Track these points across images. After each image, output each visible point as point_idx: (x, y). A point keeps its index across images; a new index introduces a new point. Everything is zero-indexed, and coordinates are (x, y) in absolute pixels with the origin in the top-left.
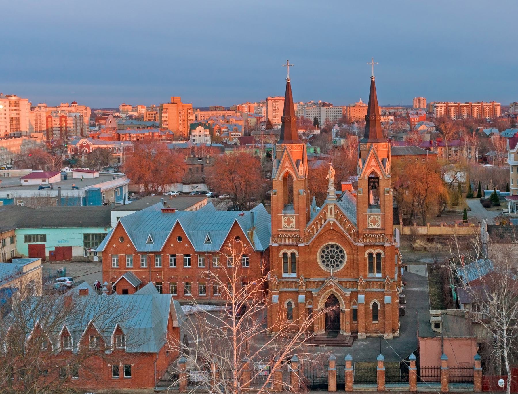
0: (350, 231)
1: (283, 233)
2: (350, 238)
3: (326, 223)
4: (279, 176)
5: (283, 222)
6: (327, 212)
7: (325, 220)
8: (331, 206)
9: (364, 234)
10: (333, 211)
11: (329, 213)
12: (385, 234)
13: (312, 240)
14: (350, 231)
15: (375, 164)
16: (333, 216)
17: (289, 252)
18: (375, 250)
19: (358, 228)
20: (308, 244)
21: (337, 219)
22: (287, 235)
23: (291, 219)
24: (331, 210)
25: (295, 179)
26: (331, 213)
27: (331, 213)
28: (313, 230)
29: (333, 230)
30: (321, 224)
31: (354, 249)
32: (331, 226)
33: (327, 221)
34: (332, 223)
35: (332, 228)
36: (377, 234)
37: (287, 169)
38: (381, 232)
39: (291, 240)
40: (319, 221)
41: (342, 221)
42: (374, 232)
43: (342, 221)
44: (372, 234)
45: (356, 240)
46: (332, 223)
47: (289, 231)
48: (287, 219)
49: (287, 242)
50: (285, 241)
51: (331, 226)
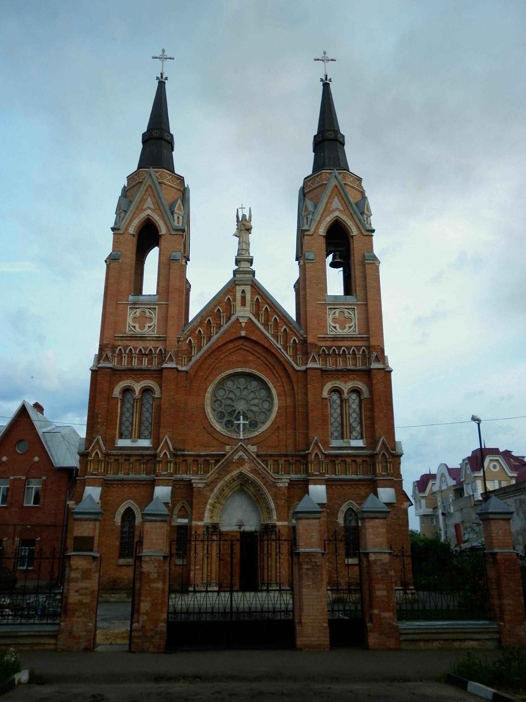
0: (286, 341)
1: (127, 343)
3: (230, 322)
4: (129, 225)
5: (129, 320)
7: (229, 318)
8: (242, 287)
9: (320, 347)
10: (248, 296)
14: (286, 341)
15: (341, 208)
16: (248, 308)
17: (138, 387)
19: (306, 333)
20: (184, 369)
21: (257, 315)
23: (148, 314)
24: (243, 299)
26: (243, 304)
27: (243, 304)
28: (199, 337)
29: (245, 338)
30: (219, 327)
31: (294, 379)
32: (241, 328)
33: (233, 318)
34: (243, 321)
35: (243, 333)
36: (349, 348)
38: (359, 343)
39: (145, 361)
40: (214, 319)
41: (267, 320)
43: (267, 320)
45: (299, 361)
46: (243, 321)
47: (142, 338)
49: (135, 364)
50: (130, 362)
51: (241, 328)
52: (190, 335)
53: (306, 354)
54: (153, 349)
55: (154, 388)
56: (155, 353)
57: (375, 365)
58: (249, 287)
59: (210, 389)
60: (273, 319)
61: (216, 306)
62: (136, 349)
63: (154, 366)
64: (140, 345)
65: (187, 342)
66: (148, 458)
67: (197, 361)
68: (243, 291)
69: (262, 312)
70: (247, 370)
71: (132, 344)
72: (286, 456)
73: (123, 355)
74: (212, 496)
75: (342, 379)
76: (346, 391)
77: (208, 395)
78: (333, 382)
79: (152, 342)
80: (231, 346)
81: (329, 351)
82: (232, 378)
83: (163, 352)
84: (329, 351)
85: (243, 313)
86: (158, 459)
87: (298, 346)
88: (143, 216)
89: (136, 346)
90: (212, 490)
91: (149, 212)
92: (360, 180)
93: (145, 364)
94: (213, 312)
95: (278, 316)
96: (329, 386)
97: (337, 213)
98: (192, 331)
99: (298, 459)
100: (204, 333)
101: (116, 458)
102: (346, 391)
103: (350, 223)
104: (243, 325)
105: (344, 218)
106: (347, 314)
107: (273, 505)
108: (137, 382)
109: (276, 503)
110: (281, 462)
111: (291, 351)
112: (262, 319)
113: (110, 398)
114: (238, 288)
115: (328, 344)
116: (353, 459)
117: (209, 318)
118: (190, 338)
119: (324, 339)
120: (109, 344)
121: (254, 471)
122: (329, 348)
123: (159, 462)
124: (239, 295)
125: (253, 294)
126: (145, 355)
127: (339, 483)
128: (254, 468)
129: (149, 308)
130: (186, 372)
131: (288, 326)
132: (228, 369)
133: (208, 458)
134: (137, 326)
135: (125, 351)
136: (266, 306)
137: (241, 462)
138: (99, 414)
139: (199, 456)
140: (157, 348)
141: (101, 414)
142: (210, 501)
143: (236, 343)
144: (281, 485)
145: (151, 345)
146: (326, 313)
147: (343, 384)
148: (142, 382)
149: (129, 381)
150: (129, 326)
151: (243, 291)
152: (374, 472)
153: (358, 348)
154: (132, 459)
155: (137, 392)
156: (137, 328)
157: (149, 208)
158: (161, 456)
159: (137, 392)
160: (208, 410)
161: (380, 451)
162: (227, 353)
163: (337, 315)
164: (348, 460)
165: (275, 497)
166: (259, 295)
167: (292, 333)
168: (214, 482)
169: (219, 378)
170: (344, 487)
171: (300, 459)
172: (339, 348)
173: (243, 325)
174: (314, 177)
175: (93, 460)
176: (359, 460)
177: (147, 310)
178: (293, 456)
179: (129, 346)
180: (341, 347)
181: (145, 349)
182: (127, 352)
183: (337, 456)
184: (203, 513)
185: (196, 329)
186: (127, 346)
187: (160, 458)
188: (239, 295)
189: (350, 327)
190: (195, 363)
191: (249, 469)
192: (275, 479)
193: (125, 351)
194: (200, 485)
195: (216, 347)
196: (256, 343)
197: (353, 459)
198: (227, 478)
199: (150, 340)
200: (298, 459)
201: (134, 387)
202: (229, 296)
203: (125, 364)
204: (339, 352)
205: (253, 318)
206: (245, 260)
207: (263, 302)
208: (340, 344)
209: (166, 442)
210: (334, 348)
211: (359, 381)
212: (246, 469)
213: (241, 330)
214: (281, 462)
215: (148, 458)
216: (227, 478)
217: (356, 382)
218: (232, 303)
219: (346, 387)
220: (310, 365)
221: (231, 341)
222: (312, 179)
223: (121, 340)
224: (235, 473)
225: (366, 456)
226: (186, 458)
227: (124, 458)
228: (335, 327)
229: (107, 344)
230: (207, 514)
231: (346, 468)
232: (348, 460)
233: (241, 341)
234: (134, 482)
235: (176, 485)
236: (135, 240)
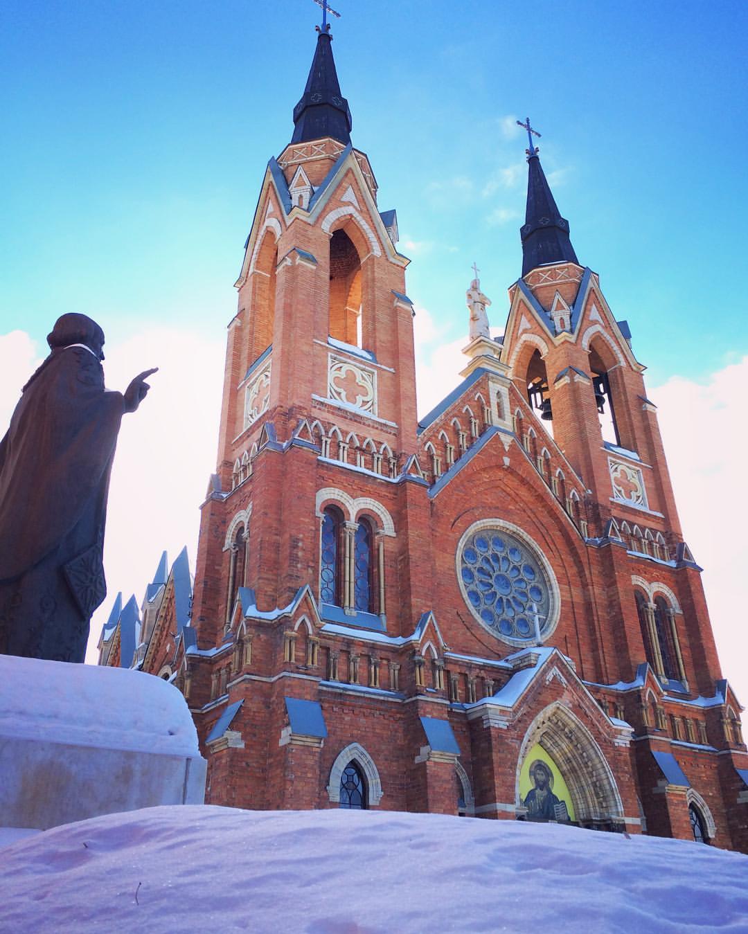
2: (566, 516)
11: (494, 409)
12: (664, 534)
22: (345, 433)
23: (359, 379)
25: (377, 252)
26: (501, 416)
27: (501, 416)
33: (489, 432)
36: (643, 529)
37: (350, 210)
47: (356, 418)
48: (342, 374)
52: (429, 440)
54: (373, 444)
55: (382, 516)
56: (378, 451)
58: (507, 389)
60: (543, 452)
62: (345, 433)
65: (426, 449)
69: (526, 437)
71: (339, 425)
73: (324, 439)
75: (644, 575)
79: (373, 432)
80: (485, 477)
83: (391, 455)
86: (417, 658)
87: (579, 506)
89: (344, 428)
94: (460, 411)
100: (451, 442)
104: (507, 448)
108: (354, 497)
109: (617, 778)
111: (570, 510)
117: (455, 419)
118: (429, 443)
120: (306, 409)
123: (420, 664)
128: (576, 703)
135: (327, 432)
136: (531, 428)
140: (381, 443)
141: (302, 540)
145: (371, 436)
146: (608, 466)
147: (646, 583)
148: (362, 500)
150: (331, 391)
153: (654, 531)
157: (350, 204)
158: (423, 654)
167: (570, 482)
172: (632, 525)
173: (507, 448)
174: (555, 269)
175: (296, 638)
177: (358, 373)
179: (334, 425)
180: (634, 524)
181: (362, 439)
182: (330, 435)
185: (438, 432)
187: (421, 655)
191: (570, 705)
193: (327, 432)
196: (523, 481)
199: (369, 426)
201: (347, 505)
202: (478, 394)
204: (632, 531)
208: (632, 518)
210: (624, 522)
211: (663, 583)
213: (504, 455)
218: (486, 408)
221: (484, 470)
222: (549, 270)
223: (320, 409)
229: (300, 407)
233: (501, 474)
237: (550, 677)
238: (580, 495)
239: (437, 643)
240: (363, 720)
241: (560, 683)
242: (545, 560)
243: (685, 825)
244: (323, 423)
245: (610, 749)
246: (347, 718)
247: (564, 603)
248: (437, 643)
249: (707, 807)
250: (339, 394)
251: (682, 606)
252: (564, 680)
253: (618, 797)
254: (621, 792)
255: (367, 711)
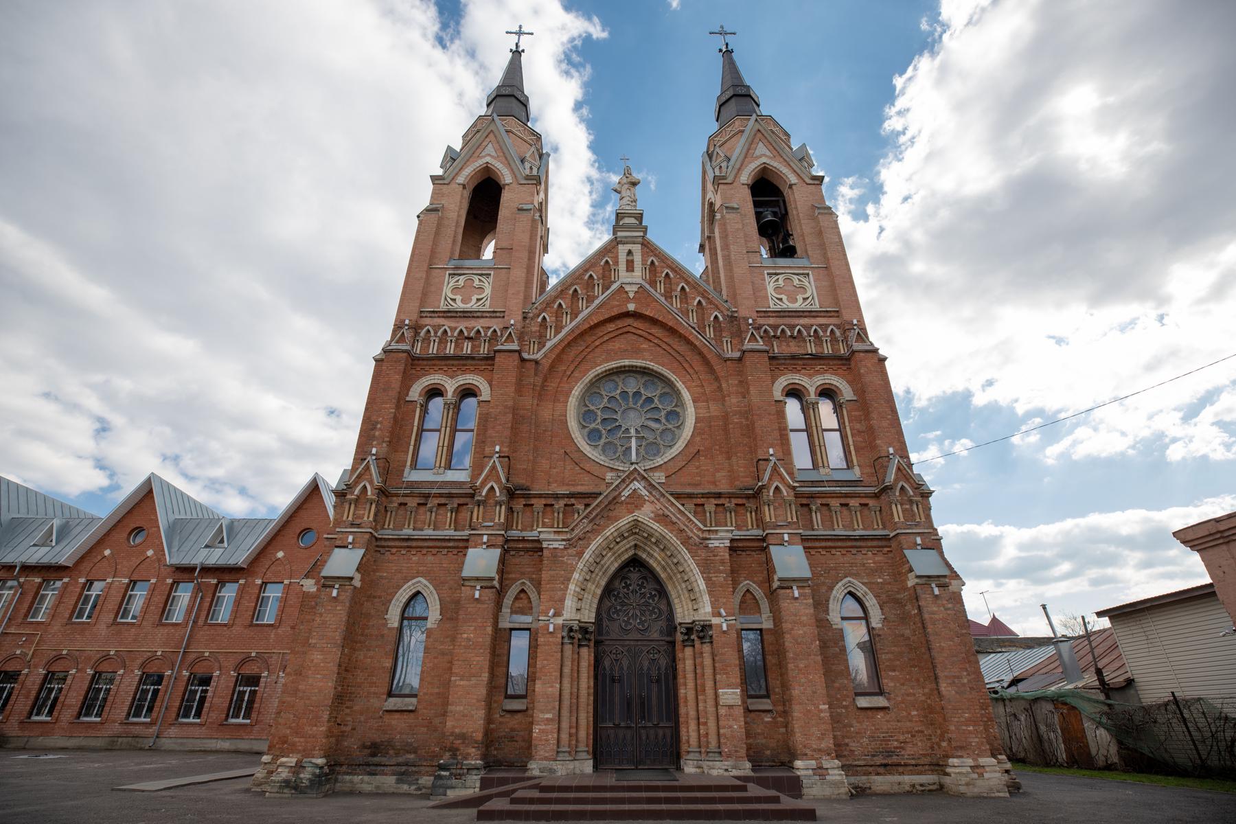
6: (616, 263)
7: (606, 288)
10: (637, 258)
11: (622, 266)
13: (549, 345)
17: (451, 386)
18: (810, 376)
21: (653, 283)
26: (630, 266)
27: (630, 266)
29: (635, 315)
31: (721, 374)
33: (614, 287)
34: (631, 290)
35: (631, 307)
36: (808, 327)
42: (796, 321)
44: (792, 327)
46: (631, 290)
49: (450, 349)
51: (629, 300)
52: (544, 310)
53: (738, 334)
57: (857, 346)
59: (577, 391)
61: (586, 271)
63: (484, 350)
64: (462, 325)
65: (540, 320)
66: (462, 501)
67: (555, 346)
68: (630, 253)
70: (639, 363)
71: (447, 324)
72: (719, 495)
74: (580, 565)
76: (812, 390)
77: (573, 402)
78: (789, 376)
80: (611, 327)
81: (775, 331)
82: (615, 377)
84: (775, 331)
85: (631, 279)
88: (478, 164)
89: (453, 325)
90: (580, 554)
91: (488, 159)
92: (788, 136)
93: (467, 348)
95: (688, 283)
96: (782, 382)
97: (764, 160)
98: (548, 304)
99: (740, 501)
101: (401, 500)
102: (812, 390)
103: (785, 170)
104: (631, 295)
105: (776, 164)
106: (796, 282)
107: (702, 584)
108: (452, 377)
109: (708, 580)
110: (710, 506)
111: (710, 333)
112: (661, 288)
113: (401, 401)
114: (620, 247)
115: (772, 321)
116: (843, 501)
119: (766, 314)
121: (662, 518)
122: (775, 327)
124: (622, 258)
125: (644, 256)
126: (469, 338)
127: (823, 544)
129: (481, 275)
130: (536, 362)
131: (704, 297)
132: (607, 361)
133: (573, 501)
134: (458, 298)
135: (436, 333)
137: (636, 501)
138: (377, 423)
139: (557, 497)
141: (381, 423)
142: (576, 575)
143: (620, 323)
144: (716, 543)
145: (479, 324)
148: (460, 378)
149: (437, 376)
151: (630, 253)
152: (887, 521)
153: (824, 327)
154: (432, 502)
155: (450, 394)
156: (459, 302)
159: (450, 394)
160: (573, 424)
161: (897, 480)
162: (606, 338)
163: (781, 282)
164: (835, 503)
165: (706, 567)
166: (655, 255)
168: (585, 538)
169: (591, 375)
170: (833, 551)
171: (744, 501)
172: (792, 327)
173: (631, 295)
176: (854, 503)
178: (730, 496)
181: (469, 329)
183: (812, 496)
184: (562, 600)
185: (554, 302)
186: (440, 326)
188: (622, 258)
189: (805, 299)
190: (551, 350)
192: (703, 531)
193: (436, 333)
194: (556, 545)
195: (587, 326)
196: (654, 321)
197: (843, 501)
198: (610, 531)
200: (740, 501)
203: (433, 349)
205: (648, 286)
206: (630, 215)
207: (661, 266)
209: (494, 467)
212: (645, 515)
214: (710, 506)
215: (462, 501)
216: (610, 531)
217: (827, 376)
218: (613, 268)
219: (811, 383)
220: (748, 345)
224: (625, 521)
225: (867, 496)
226: (533, 501)
227: (418, 500)
228: (781, 300)
230: (570, 603)
231: (831, 517)
232: (835, 503)
233: (629, 321)
234: (431, 544)
235: (509, 549)
236: (467, 194)
237: (626, 493)
238: (723, 316)
239: (498, 480)
240: (430, 558)
241: (640, 496)
242: (680, 385)
243: (804, 618)
244: (433, 326)
245: (703, 553)
246: (414, 558)
247: (698, 420)
248: (498, 480)
249: (870, 596)
250: (478, 300)
251: (855, 392)
252: (644, 492)
253: (706, 598)
254: (710, 593)
255: (434, 551)
